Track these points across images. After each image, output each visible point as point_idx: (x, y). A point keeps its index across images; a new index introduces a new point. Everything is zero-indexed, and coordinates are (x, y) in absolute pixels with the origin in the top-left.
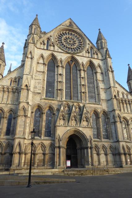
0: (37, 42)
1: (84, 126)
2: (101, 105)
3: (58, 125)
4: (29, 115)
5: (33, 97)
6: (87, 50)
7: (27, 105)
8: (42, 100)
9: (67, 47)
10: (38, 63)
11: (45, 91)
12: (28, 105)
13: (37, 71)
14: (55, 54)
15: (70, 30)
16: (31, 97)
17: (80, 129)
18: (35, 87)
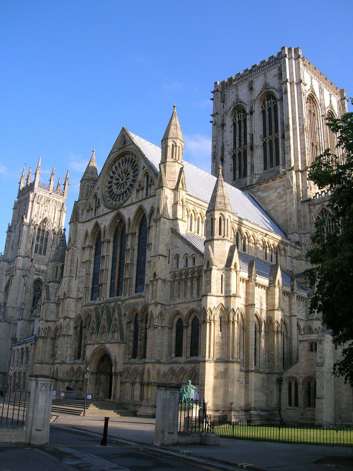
0: (83, 212)
1: (113, 341)
2: (144, 297)
3: (89, 342)
4: (71, 332)
5: (75, 307)
6: (140, 185)
7: (63, 321)
8: (83, 308)
9: (118, 195)
10: (84, 249)
11: (90, 290)
12: (68, 320)
13: (82, 262)
14: (99, 221)
15: (123, 155)
16: (74, 306)
17: (108, 345)
18: (78, 291)
